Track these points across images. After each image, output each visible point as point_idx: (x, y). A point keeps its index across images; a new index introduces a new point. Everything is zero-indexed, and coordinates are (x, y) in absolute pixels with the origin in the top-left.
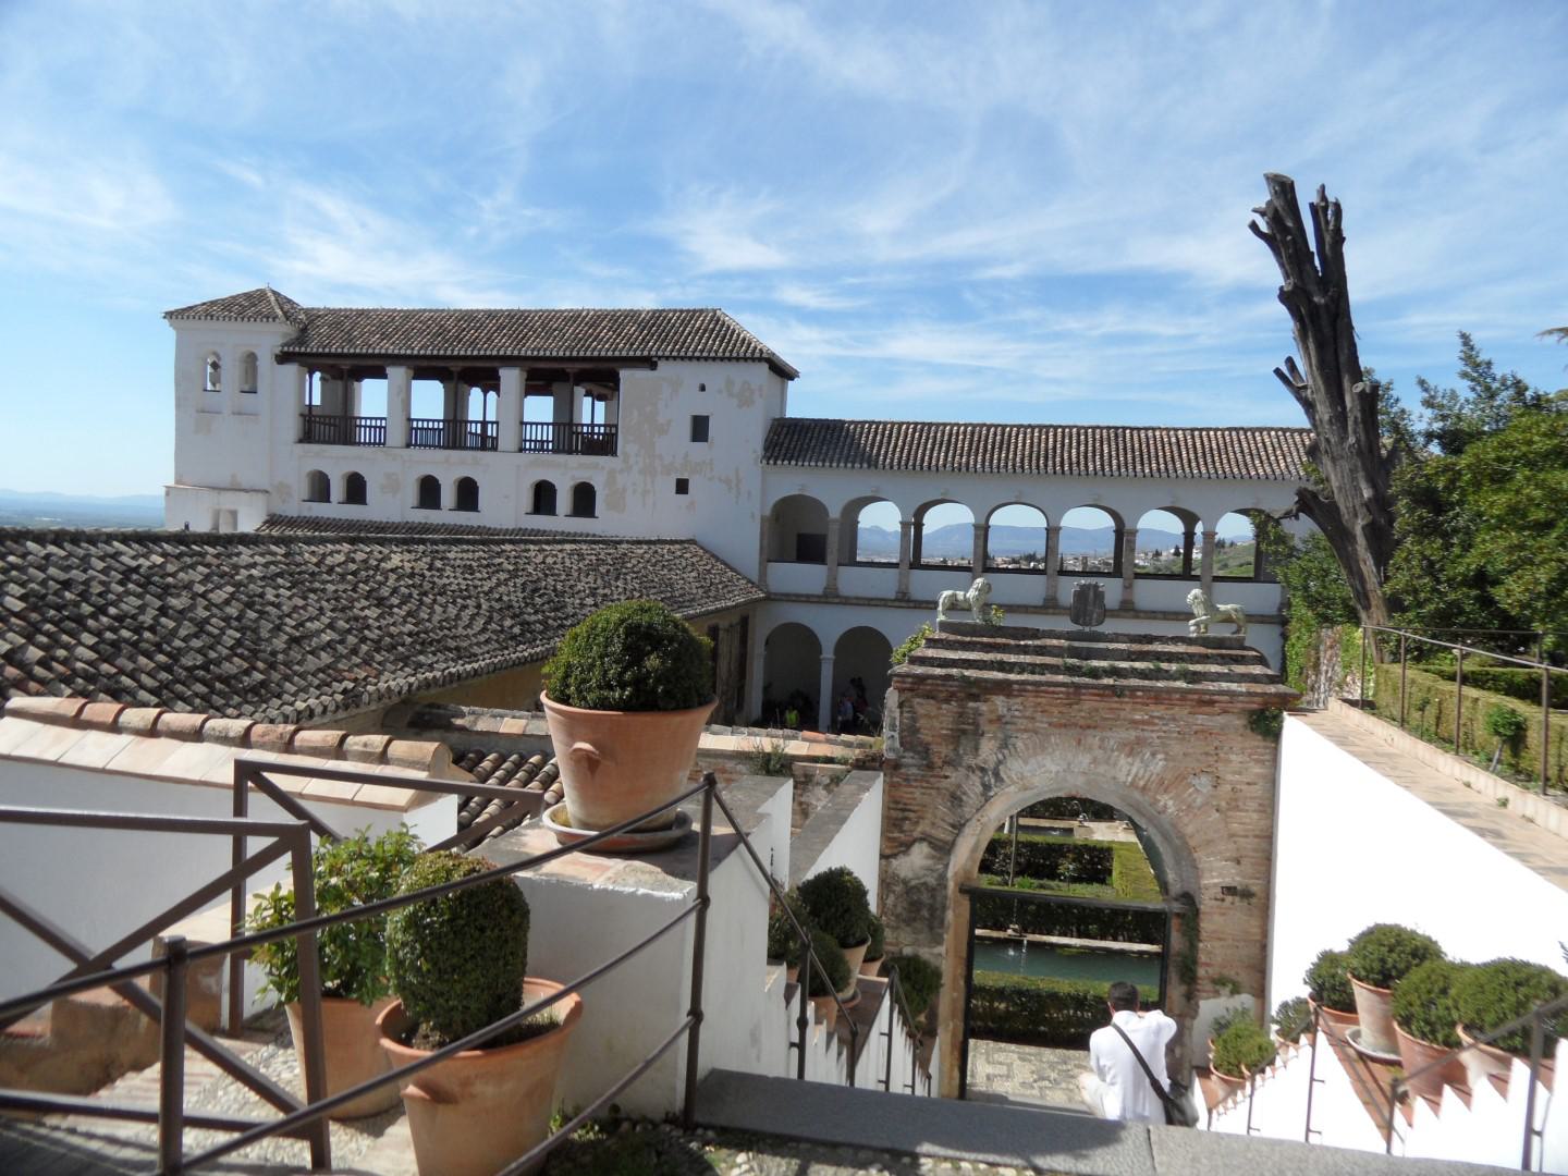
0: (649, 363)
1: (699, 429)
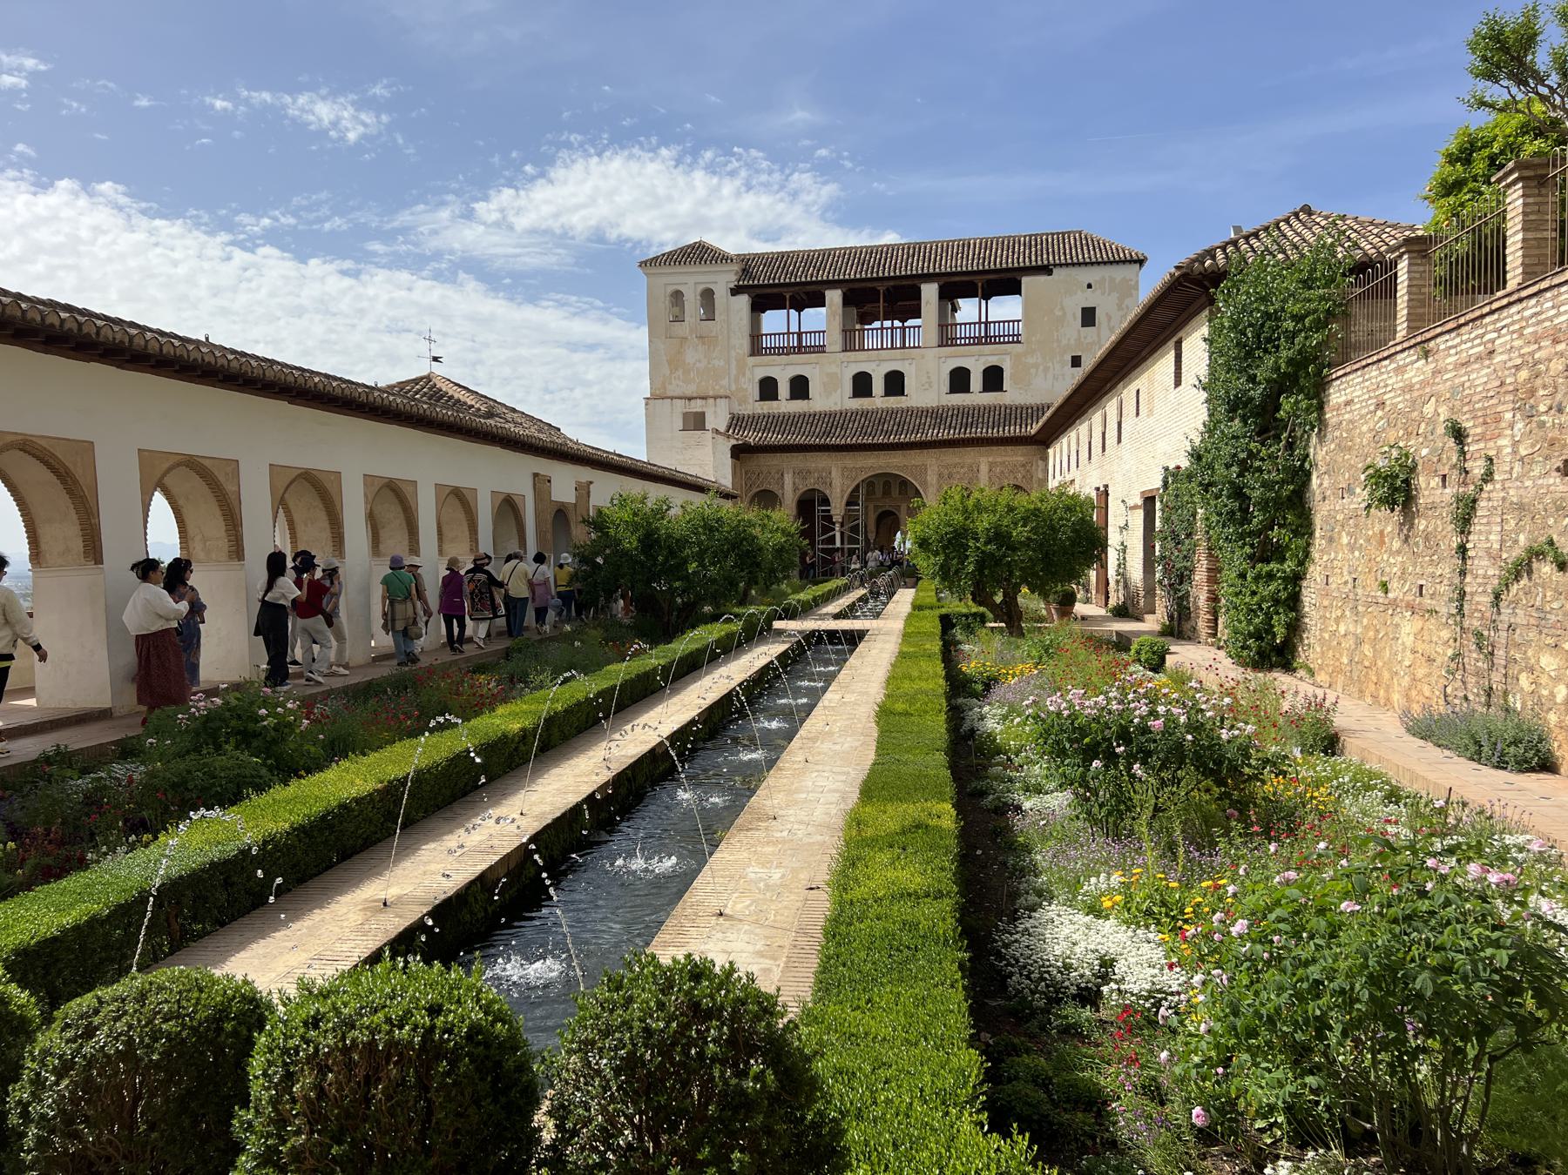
0: (1046, 270)
1: (1089, 317)
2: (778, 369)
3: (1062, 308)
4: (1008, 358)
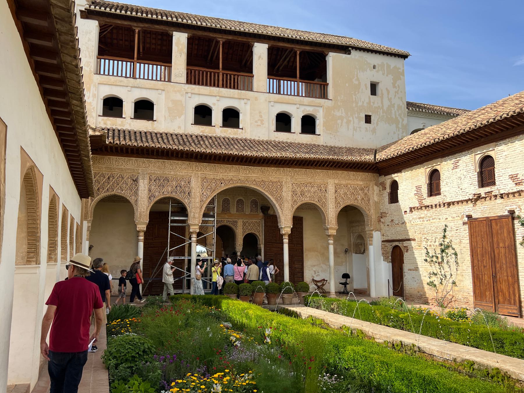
1: (374, 88)
2: (125, 90)
3: (358, 79)
4: (321, 110)
